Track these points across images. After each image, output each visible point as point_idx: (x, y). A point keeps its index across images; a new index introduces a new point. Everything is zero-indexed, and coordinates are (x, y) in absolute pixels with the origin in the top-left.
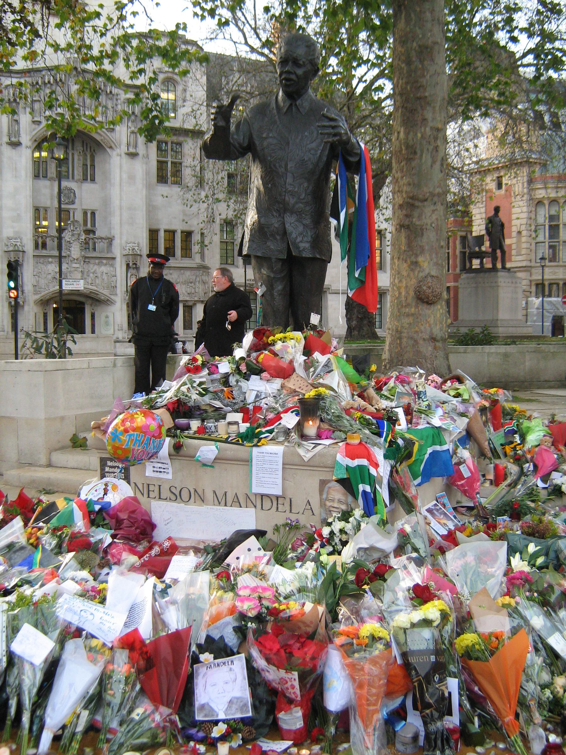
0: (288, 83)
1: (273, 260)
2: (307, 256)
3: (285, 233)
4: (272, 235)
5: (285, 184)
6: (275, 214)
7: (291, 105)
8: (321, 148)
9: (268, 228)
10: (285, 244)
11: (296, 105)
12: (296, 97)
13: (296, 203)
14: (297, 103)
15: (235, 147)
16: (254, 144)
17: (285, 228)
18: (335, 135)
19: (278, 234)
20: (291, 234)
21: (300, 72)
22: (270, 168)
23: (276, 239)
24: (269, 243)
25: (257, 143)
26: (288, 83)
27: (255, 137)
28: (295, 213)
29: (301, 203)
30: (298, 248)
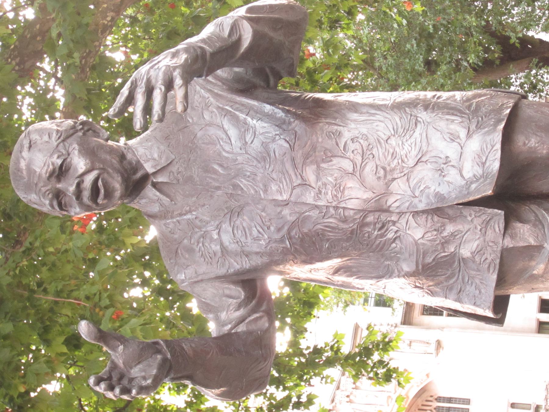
0: (102, 191)
1: (509, 243)
2: (499, 154)
3: (439, 211)
4: (446, 242)
5: (317, 207)
6: (390, 235)
7: (155, 185)
8: (242, 116)
9: (425, 254)
10: (467, 211)
11: (154, 174)
12: (139, 175)
13: (362, 182)
14: (150, 170)
15: (241, 320)
16: (237, 273)
17: (423, 212)
18: (169, 85)
19: (439, 231)
20: (439, 197)
21: (80, 164)
22: (282, 240)
23: (453, 235)
24: (465, 252)
25: (237, 265)
26: (102, 191)
27: (222, 271)
28: (388, 185)
29: (362, 168)
30: (476, 179)
